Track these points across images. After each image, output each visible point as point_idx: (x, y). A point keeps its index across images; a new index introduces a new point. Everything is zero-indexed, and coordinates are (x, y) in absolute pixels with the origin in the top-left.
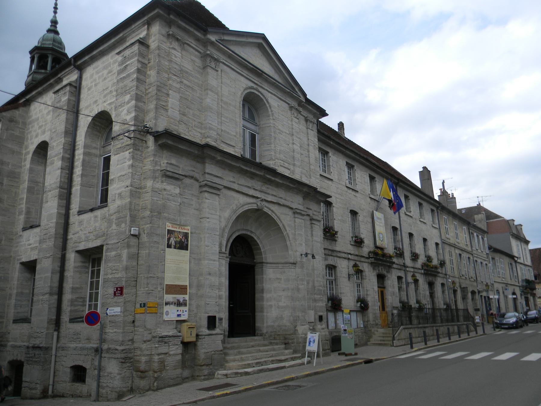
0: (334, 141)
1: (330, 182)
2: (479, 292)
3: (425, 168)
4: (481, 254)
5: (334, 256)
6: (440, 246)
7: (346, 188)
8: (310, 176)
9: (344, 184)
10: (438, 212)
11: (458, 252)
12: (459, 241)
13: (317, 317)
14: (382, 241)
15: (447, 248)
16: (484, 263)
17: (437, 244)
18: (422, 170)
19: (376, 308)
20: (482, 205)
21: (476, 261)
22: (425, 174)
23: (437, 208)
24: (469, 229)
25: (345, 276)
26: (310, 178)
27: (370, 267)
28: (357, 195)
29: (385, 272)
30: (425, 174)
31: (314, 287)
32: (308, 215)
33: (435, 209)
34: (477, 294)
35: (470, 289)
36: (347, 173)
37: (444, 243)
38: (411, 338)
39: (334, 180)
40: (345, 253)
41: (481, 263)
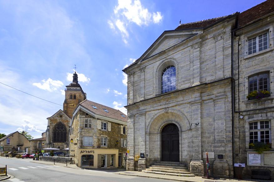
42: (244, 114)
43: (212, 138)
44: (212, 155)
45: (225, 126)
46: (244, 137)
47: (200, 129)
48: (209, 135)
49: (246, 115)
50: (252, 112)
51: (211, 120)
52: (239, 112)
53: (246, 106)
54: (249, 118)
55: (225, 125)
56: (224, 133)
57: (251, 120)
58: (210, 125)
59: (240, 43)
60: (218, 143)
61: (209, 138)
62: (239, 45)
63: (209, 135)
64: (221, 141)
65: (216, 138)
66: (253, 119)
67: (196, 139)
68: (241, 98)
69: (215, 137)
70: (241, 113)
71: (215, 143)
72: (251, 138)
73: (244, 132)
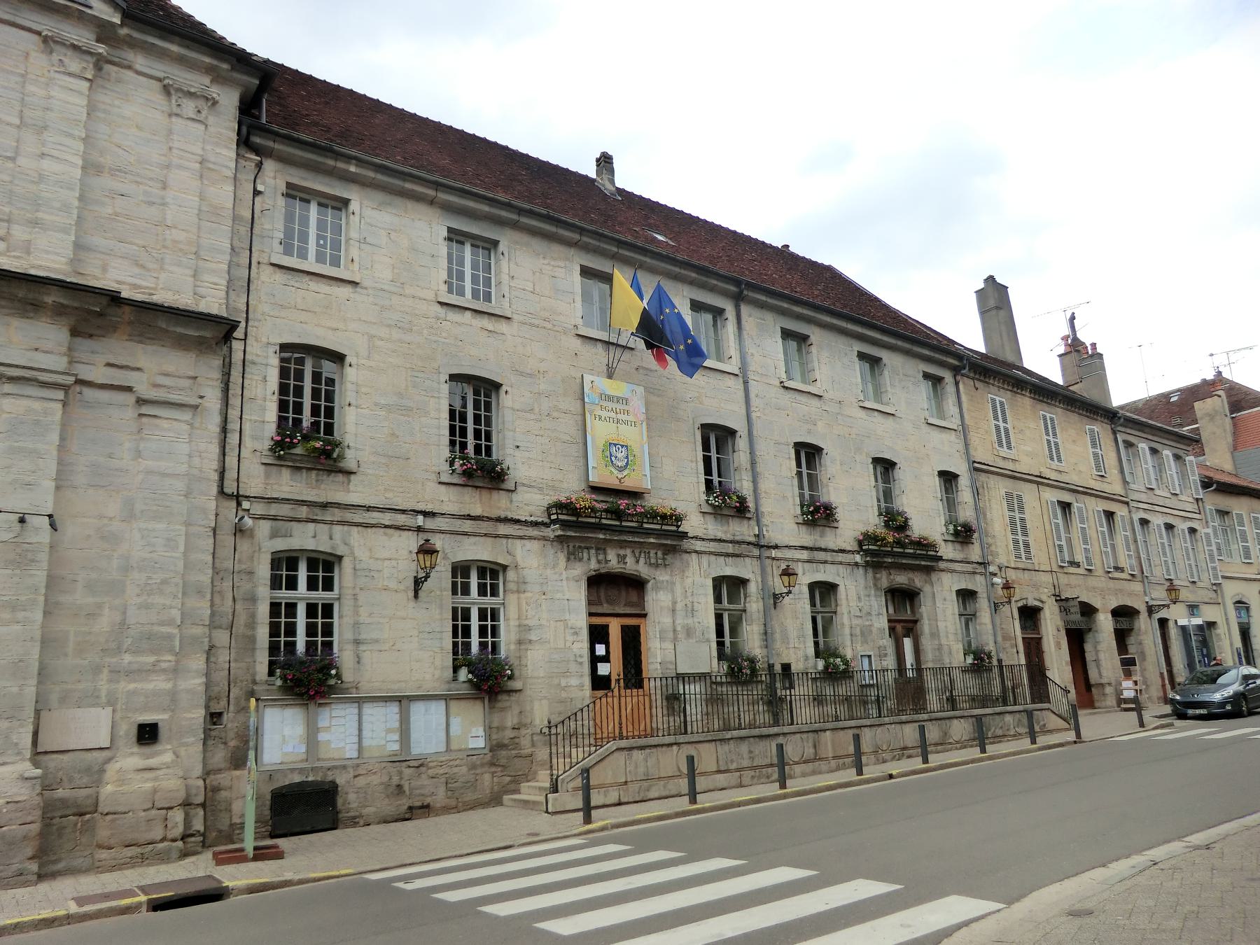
0: (360, 162)
1: (345, 291)
2: (1151, 610)
3: (991, 280)
4: (1172, 502)
5: (332, 523)
6: (964, 482)
7: (441, 311)
8: (161, 261)
9: (430, 295)
10: (957, 384)
11: (1052, 496)
12: (1063, 466)
13: (128, 730)
14: (621, 469)
15: (998, 489)
16: (1183, 526)
17: (948, 478)
18: (981, 285)
19: (574, 682)
20: (1224, 375)
21: (1144, 522)
22: (994, 299)
23: (956, 371)
24: (1114, 433)
25: (393, 585)
26: (162, 268)
27: (550, 551)
28: (502, 327)
29: (633, 565)
30: (994, 299)
31: (123, 624)
32: (129, 389)
33: (948, 376)
34: (1144, 615)
35: (1105, 605)
36: (444, 263)
37: (978, 469)
38: (692, 775)
39: (365, 283)
40: (403, 512)
41: (1169, 527)
42: (259, 509)
43: (105, 623)
44: (89, 727)
45: (185, 553)
46: (252, 624)
47: (44, 557)
48: (90, 600)
49: (263, 517)
50: (285, 510)
51: (114, 508)
52: (238, 498)
53: (267, 476)
54: (274, 535)
55: (182, 549)
56: (175, 597)
57: (281, 544)
58: (103, 538)
59: (260, 188)
60: (137, 652)
61: (92, 616)
62: (256, 193)
63: (90, 600)
64: (152, 641)
65: (131, 620)
66: (289, 540)
67: (6, 615)
68: (247, 427)
69: (124, 613)
70: (246, 505)
71: (119, 650)
72: (274, 631)
73: (253, 599)
